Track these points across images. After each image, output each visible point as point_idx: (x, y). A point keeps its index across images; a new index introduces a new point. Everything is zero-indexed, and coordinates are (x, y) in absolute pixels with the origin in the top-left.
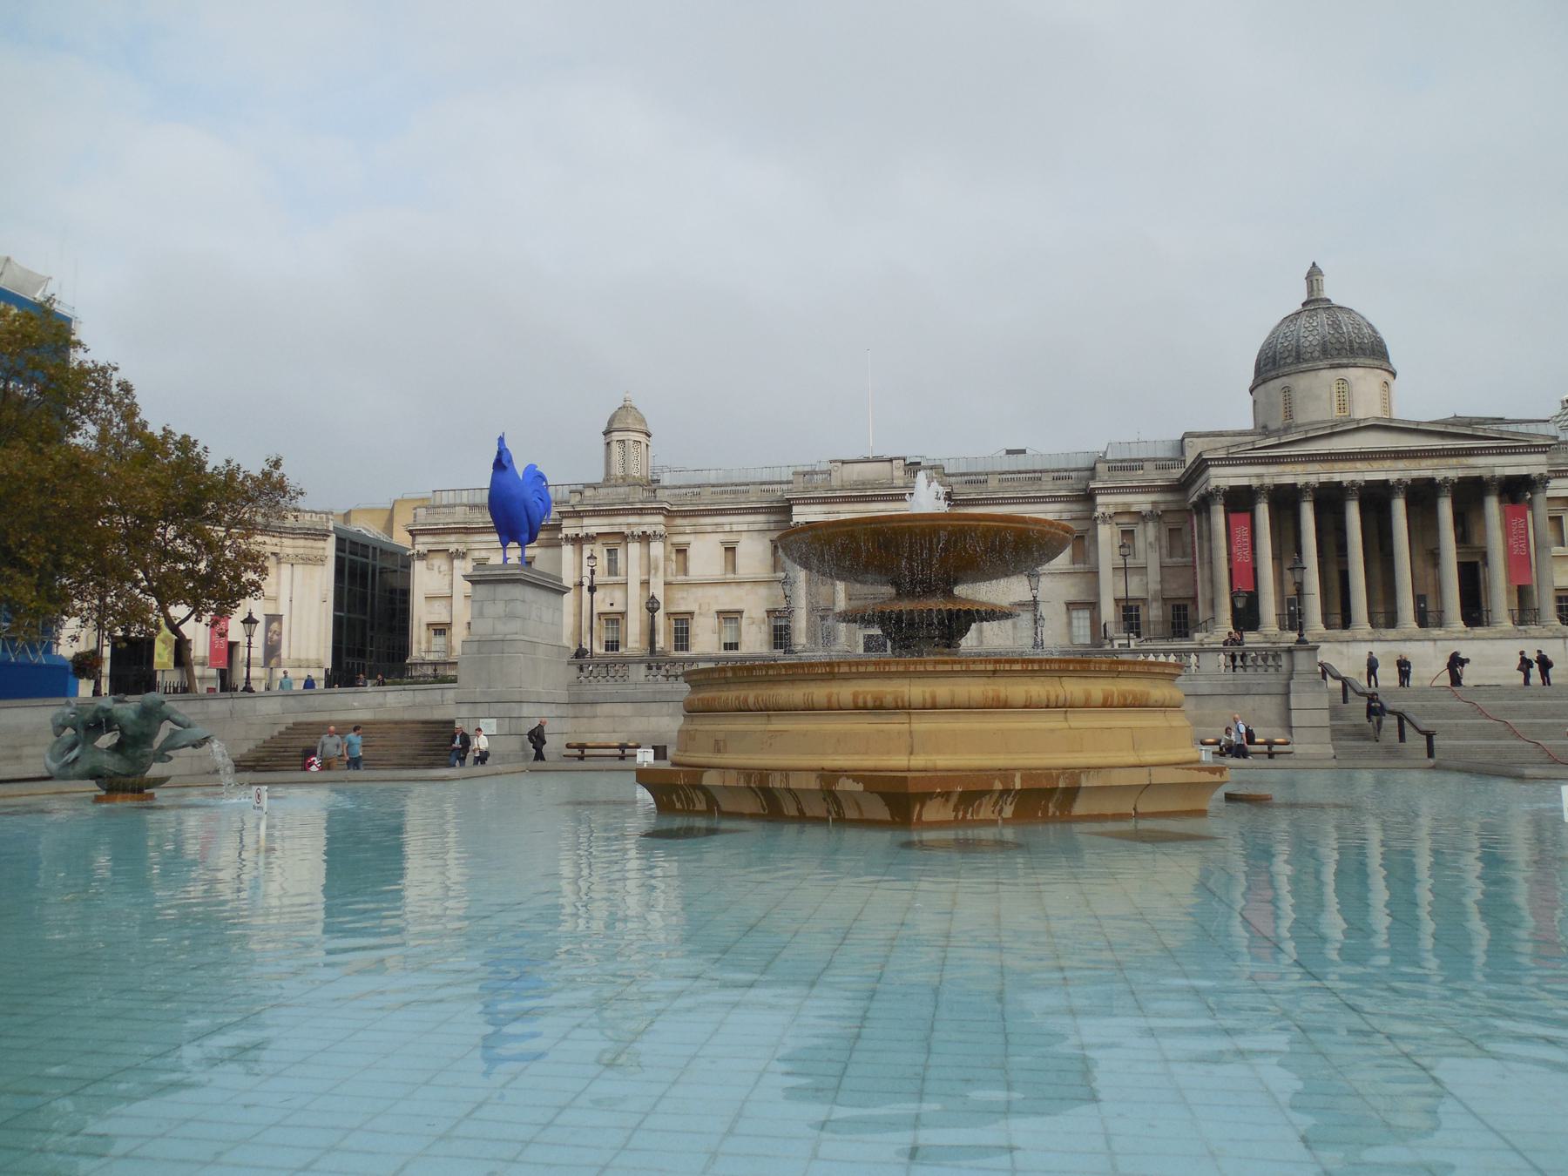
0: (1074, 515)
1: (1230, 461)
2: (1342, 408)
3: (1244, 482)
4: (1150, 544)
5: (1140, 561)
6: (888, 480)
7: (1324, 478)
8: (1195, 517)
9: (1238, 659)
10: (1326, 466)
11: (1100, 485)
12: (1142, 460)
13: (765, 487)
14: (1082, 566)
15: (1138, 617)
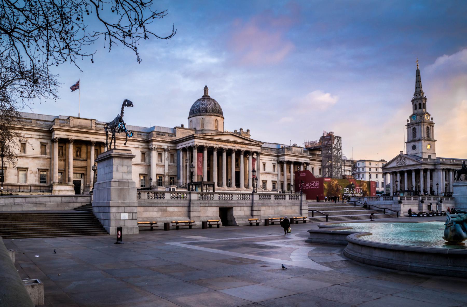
0: (143, 147)
1: (200, 138)
2: (216, 127)
3: (202, 144)
4: (166, 158)
5: (163, 163)
6: (90, 127)
7: (220, 146)
8: (181, 153)
9: (278, 197)
10: (220, 143)
11: (154, 139)
12: (165, 133)
13: (38, 122)
14: (144, 163)
15: (161, 180)
